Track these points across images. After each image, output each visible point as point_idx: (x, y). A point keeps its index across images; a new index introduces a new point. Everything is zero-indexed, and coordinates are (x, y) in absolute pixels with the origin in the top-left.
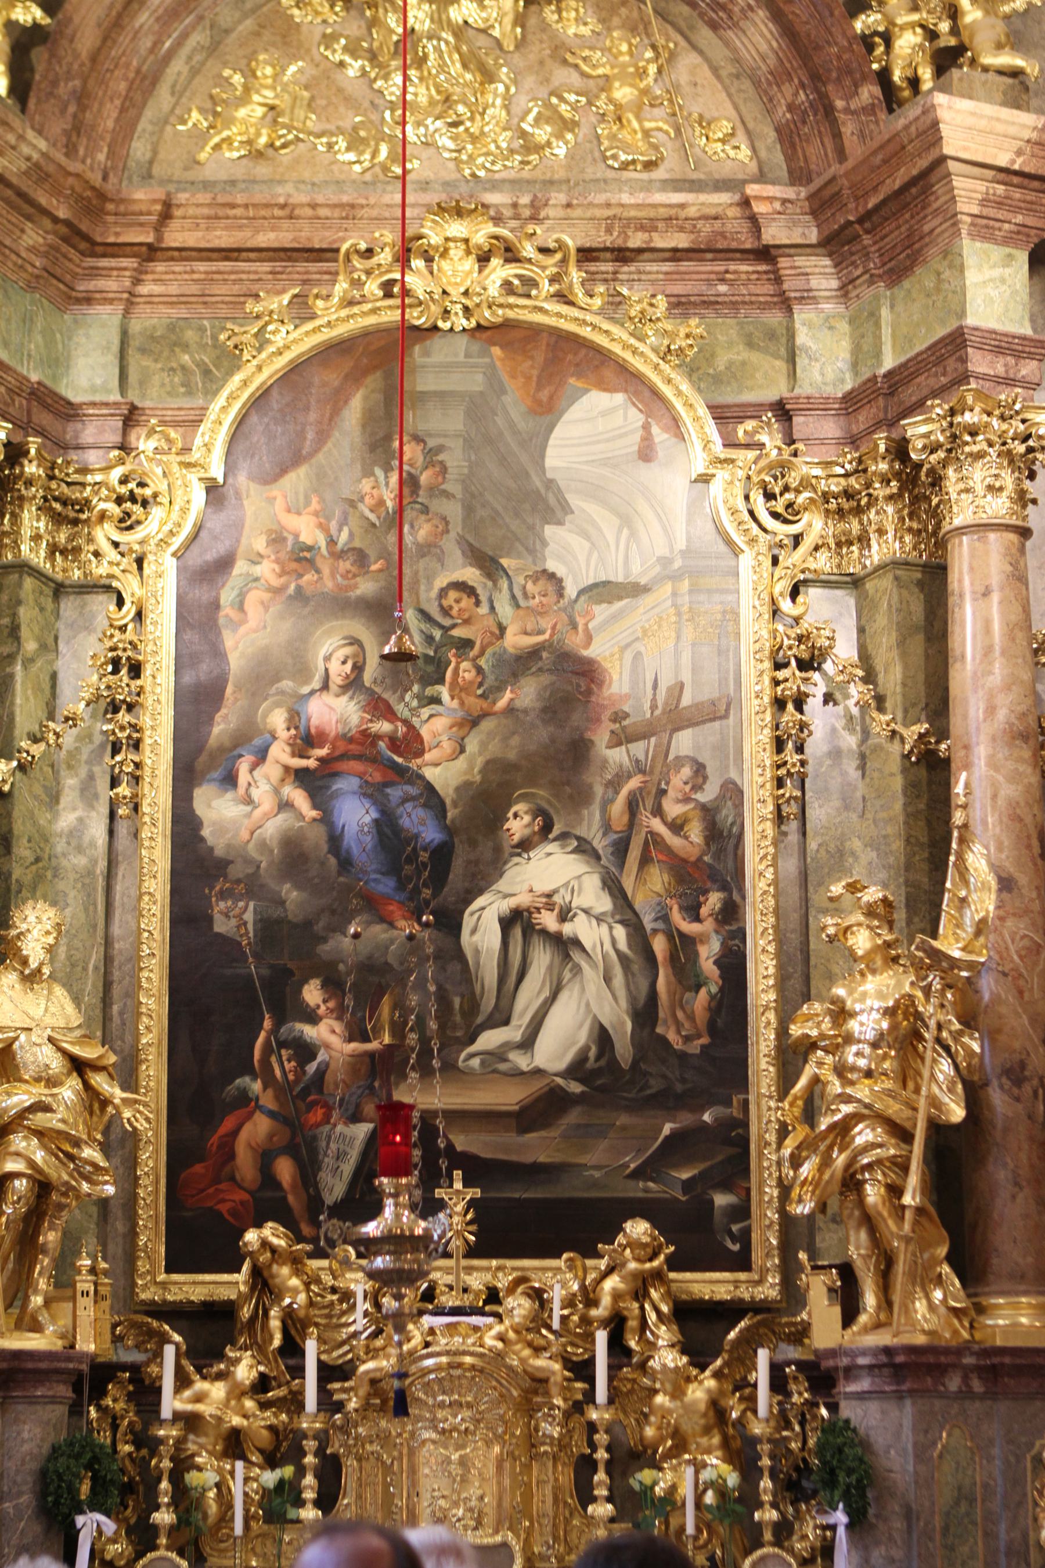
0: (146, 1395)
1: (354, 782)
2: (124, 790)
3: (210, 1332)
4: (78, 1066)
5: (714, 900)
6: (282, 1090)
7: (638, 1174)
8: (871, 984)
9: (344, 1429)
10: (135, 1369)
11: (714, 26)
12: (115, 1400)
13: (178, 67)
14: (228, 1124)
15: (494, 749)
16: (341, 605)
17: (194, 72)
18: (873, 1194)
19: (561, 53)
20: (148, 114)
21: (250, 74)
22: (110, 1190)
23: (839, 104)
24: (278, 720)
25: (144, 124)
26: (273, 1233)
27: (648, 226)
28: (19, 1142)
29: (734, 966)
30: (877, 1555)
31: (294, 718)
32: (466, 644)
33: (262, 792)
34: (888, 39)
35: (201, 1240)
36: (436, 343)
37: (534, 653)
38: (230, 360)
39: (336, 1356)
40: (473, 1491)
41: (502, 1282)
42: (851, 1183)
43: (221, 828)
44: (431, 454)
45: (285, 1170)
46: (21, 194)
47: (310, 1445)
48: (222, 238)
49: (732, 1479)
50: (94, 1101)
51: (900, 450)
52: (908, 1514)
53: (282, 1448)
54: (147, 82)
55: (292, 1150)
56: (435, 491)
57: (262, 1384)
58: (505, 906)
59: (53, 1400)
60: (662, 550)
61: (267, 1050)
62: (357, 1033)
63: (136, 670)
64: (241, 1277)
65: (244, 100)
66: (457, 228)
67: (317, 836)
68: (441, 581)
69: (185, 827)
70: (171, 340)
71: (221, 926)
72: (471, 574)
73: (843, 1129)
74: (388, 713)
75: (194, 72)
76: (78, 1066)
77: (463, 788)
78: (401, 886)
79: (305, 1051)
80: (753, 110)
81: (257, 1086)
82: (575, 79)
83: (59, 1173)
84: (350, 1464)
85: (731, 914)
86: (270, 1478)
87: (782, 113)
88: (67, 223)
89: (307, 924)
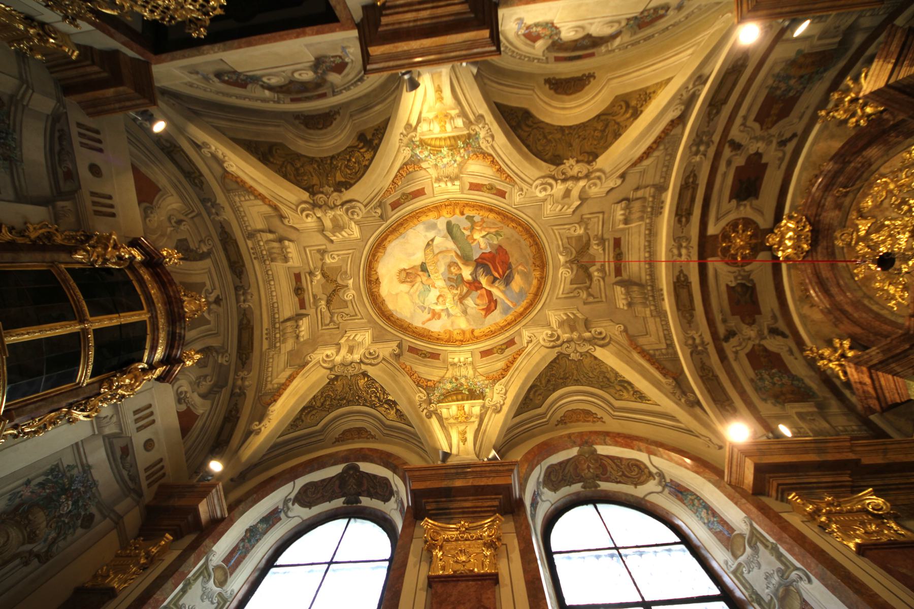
11: (870, 165)
13: (875, 308)
17: (877, 303)
19: (878, 206)
20: (889, 317)
21: (878, 289)
23: (891, 123)
25: (893, 318)
46: (893, 357)
54: (878, 316)
65: (887, 291)
75: (877, 303)
82: (887, 201)
87: (900, 138)
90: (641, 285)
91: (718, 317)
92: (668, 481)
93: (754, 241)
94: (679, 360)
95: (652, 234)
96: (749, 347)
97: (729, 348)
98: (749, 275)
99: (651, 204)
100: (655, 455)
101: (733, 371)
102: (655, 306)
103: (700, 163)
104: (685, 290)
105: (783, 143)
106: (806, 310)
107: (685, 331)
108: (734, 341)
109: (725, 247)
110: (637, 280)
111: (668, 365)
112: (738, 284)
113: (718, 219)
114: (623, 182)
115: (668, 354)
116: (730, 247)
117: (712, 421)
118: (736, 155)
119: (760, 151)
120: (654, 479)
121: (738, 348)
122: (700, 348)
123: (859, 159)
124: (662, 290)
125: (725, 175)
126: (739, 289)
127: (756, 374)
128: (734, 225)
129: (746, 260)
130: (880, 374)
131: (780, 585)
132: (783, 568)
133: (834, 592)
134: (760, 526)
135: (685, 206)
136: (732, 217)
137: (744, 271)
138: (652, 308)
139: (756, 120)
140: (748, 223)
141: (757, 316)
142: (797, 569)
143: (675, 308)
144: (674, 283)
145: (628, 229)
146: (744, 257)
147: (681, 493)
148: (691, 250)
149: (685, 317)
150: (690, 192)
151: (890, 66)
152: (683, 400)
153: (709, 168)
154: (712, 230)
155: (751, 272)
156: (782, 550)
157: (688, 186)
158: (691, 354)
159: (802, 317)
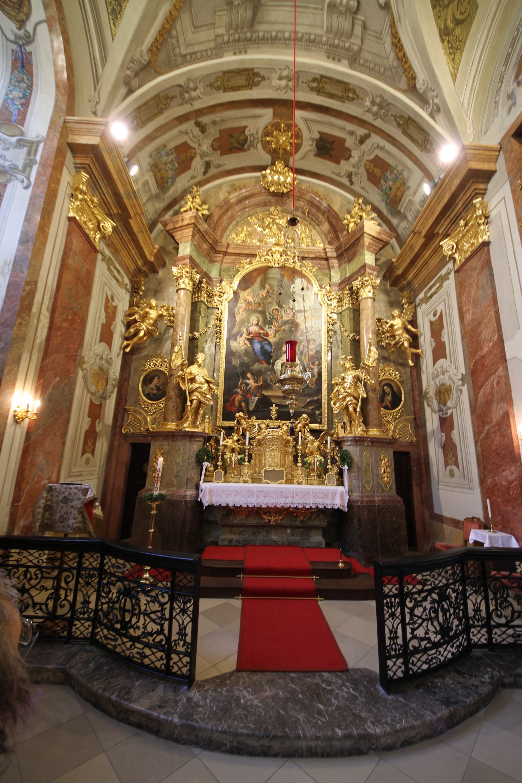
0: (217, 441)
1: (257, 341)
2: (218, 340)
3: (229, 431)
4: (208, 382)
5: (317, 363)
6: (243, 391)
7: (303, 407)
8: (349, 373)
9: (253, 449)
10: (216, 437)
11: (318, 225)
12: (212, 442)
13: (231, 227)
14: (234, 397)
15: (281, 336)
16: (256, 311)
17: (233, 228)
18: (351, 409)
22: (212, 403)
24: (244, 330)
25: (225, 236)
26: (241, 414)
27: (308, 253)
28: (196, 393)
29: (320, 374)
30: (352, 475)
31: (247, 330)
32: (276, 319)
33: (241, 342)
34: (348, 225)
35: (228, 416)
36: (273, 269)
37: (288, 321)
38: (238, 271)
39: (253, 435)
40: (276, 460)
41: (281, 424)
42: (347, 407)
43: (234, 347)
44: (271, 288)
45: (243, 404)
46: (203, 235)
47: (247, 451)
48: (237, 251)
49: (323, 460)
50: (210, 389)
51: (351, 289)
52: (358, 467)
53: (242, 452)
54: (225, 229)
55: (244, 401)
56: (272, 294)
57: (238, 440)
58: (282, 362)
59: (200, 441)
60: (309, 305)
61: (241, 384)
62: (256, 382)
63: (221, 321)
64: (235, 422)
66: (278, 248)
67: (251, 349)
68: (273, 308)
69: (228, 347)
70: (228, 270)
71: (234, 363)
72: (277, 307)
73: (344, 398)
74: (263, 329)
75: (233, 228)
76: (208, 382)
77: (275, 342)
78: (265, 358)
79: (247, 385)
80: (324, 239)
81: (239, 390)
83: (202, 399)
84: (253, 455)
85: (320, 364)
86: (239, 457)
87: (329, 239)
88: (211, 244)
89: (248, 364)
90: (253, 22)
91: (217, 116)
92: (29, 48)
93: (281, 152)
94: (171, 71)
95: (310, 43)
96: (193, 145)
97: (190, 125)
98: (254, 147)
99: (342, 44)
101: (170, 129)
102: (228, 42)
103: (362, 106)
104: (244, 82)
105: (350, 176)
106: (225, 189)
107: (202, 79)
108: (197, 131)
109: (280, 126)
110: (258, 18)
111: (162, 56)
112: (247, 137)
113: (306, 120)
114: (380, 6)
115: (175, 55)
116: (280, 130)
117: (118, 105)
118: (356, 140)
119: (351, 159)
120: (19, 29)
121: (191, 135)
122: (187, 96)
123: (324, 220)
124: (246, 52)
125: (343, 129)
126: (242, 138)
127: (171, 150)
128: (298, 136)
129: (266, 145)
130: (192, 229)
132: (20, 168)
133: (29, 204)
135: (328, 88)
136: (305, 134)
137: (257, 143)
138: (226, 38)
139: (377, 156)
140: (297, 147)
141: (219, 152)
143: (225, 68)
144: (252, 69)
145: (322, 9)
146: (268, 142)
147: (23, 66)
148: (284, 91)
149: (217, 80)
150: (340, 94)
151: (374, 234)
152: (128, 72)
153: (354, 114)
154: (299, 114)
155: (256, 148)
156: (35, 168)
157: (346, 90)
158: (179, 86)
159: (220, 186)
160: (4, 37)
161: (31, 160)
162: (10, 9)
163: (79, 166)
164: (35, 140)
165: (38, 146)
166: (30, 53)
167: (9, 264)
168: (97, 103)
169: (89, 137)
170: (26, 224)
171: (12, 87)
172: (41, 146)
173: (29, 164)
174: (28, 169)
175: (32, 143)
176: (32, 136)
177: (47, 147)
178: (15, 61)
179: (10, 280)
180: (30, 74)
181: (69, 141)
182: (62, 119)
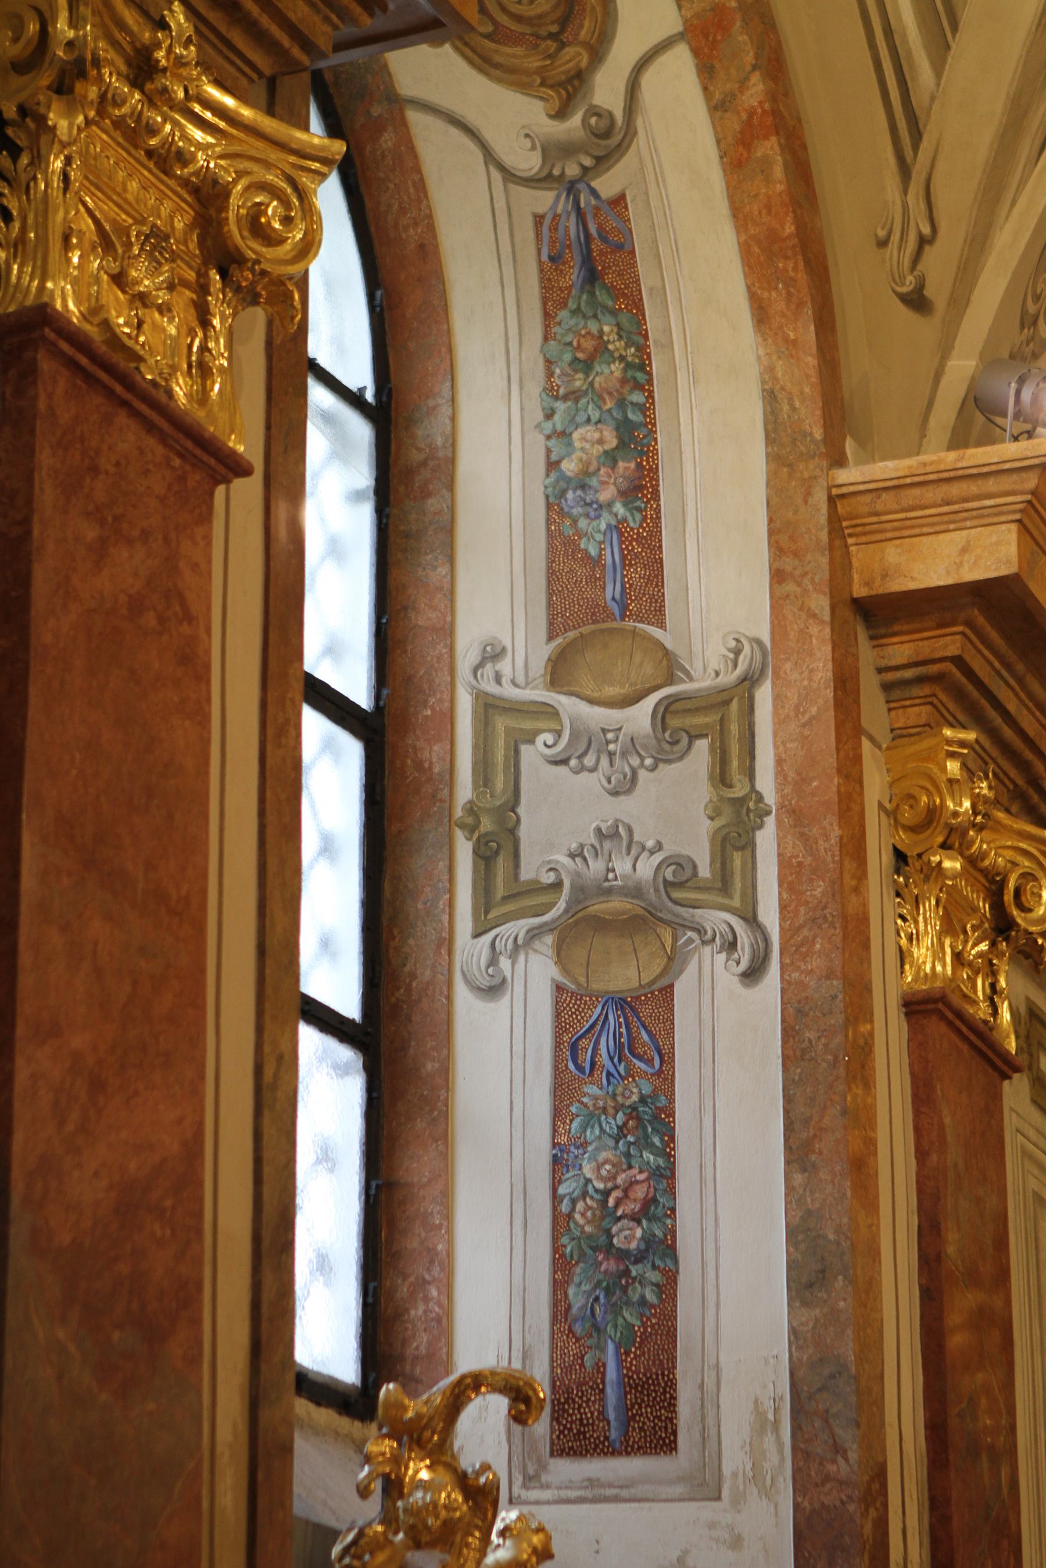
92: (607, 185)
100: (706, 71)
120: (561, 114)
131: (635, 892)
132: (705, 871)
134: (779, 721)
142: (752, 920)
147: (592, 277)
156: (767, 840)
160: (496, 175)
161: (741, 801)
162: (518, 50)
163: (908, 674)
164: (729, 678)
165: (749, 709)
166: (619, 201)
167: (776, 1423)
168: (923, 242)
169: (959, 537)
170: (798, 1178)
171: (561, 406)
172: (764, 695)
173: (734, 840)
174: (737, 859)
175: (718, 701)
176: (714, 664)
177: (792, 696)
178: (554, 261)
179: (796, 1507)
180: (631, 302)
181: (859, 591)
182: (820, 497)
